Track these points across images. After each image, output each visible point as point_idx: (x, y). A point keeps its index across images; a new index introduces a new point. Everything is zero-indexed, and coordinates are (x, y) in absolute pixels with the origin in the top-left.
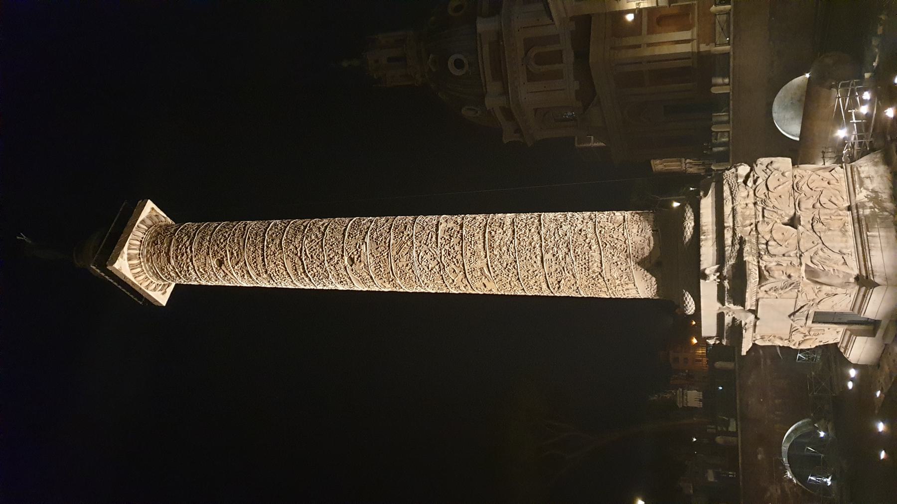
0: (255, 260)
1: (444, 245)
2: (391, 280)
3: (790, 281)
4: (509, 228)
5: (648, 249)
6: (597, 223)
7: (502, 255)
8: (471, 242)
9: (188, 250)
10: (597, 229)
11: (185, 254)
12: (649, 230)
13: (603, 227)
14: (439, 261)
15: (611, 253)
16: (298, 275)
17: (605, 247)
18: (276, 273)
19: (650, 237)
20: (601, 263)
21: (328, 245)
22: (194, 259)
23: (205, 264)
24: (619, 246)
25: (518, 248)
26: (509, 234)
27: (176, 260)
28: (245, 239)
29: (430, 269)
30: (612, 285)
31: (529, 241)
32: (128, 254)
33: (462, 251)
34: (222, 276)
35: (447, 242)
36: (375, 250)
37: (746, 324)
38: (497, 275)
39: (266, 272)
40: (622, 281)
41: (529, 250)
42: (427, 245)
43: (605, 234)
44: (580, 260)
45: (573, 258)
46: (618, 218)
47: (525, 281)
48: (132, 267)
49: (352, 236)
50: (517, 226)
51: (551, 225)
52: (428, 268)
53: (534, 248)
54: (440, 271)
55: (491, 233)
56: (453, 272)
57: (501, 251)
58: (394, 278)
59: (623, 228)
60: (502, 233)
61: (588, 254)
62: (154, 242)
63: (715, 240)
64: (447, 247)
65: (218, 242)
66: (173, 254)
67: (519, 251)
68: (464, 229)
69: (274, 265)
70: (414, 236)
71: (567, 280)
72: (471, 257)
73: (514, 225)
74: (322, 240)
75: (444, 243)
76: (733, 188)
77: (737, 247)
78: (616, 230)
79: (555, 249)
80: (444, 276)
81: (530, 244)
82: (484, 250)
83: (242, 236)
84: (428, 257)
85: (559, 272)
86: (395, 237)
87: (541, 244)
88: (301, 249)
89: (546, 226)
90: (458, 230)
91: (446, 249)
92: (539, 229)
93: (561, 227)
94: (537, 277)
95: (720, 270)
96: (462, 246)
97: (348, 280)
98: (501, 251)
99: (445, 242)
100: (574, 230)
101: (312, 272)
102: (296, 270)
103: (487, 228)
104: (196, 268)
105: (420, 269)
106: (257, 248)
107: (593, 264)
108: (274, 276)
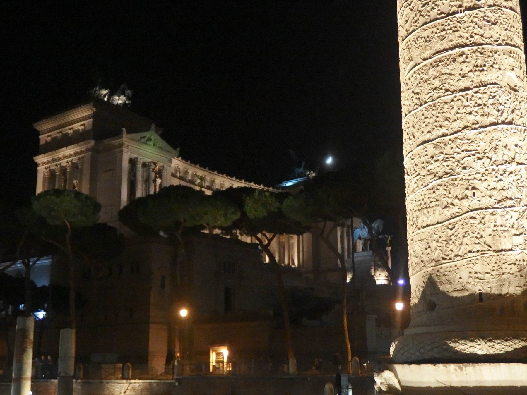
4: (472, 81)
6: (491, 211)
7: (429, 82)
8: (444, 30)
10: (478, 212)
12: (480, 288)
13: (483, 221)
15: (440, 237)
17: (448, 228)
19: (467, 290)
20: (428, 226)
25: (439, 102)
31: (451, 116)
33: (431, 22)
41: (437, 119)
43: (469, 226)
44: (430, 196)
50: (477, 92)
51: (482, 144)
53: (441, 127)
55: (461, 55)
59: (485, 251)
60: (461, 72)
63: (448, 385)
67: (434, 106)
68: (467, 12)
78: (477, 241)
79: (441, 157)
87: (447, 135)
89: (481, 136)
90: (465, 5)
92: (474, 126)
93: (479, 159)
96: (437, 19)
98: (434, 79)
100: (475, 178)
103: (470, 48)
107: (425, 214)
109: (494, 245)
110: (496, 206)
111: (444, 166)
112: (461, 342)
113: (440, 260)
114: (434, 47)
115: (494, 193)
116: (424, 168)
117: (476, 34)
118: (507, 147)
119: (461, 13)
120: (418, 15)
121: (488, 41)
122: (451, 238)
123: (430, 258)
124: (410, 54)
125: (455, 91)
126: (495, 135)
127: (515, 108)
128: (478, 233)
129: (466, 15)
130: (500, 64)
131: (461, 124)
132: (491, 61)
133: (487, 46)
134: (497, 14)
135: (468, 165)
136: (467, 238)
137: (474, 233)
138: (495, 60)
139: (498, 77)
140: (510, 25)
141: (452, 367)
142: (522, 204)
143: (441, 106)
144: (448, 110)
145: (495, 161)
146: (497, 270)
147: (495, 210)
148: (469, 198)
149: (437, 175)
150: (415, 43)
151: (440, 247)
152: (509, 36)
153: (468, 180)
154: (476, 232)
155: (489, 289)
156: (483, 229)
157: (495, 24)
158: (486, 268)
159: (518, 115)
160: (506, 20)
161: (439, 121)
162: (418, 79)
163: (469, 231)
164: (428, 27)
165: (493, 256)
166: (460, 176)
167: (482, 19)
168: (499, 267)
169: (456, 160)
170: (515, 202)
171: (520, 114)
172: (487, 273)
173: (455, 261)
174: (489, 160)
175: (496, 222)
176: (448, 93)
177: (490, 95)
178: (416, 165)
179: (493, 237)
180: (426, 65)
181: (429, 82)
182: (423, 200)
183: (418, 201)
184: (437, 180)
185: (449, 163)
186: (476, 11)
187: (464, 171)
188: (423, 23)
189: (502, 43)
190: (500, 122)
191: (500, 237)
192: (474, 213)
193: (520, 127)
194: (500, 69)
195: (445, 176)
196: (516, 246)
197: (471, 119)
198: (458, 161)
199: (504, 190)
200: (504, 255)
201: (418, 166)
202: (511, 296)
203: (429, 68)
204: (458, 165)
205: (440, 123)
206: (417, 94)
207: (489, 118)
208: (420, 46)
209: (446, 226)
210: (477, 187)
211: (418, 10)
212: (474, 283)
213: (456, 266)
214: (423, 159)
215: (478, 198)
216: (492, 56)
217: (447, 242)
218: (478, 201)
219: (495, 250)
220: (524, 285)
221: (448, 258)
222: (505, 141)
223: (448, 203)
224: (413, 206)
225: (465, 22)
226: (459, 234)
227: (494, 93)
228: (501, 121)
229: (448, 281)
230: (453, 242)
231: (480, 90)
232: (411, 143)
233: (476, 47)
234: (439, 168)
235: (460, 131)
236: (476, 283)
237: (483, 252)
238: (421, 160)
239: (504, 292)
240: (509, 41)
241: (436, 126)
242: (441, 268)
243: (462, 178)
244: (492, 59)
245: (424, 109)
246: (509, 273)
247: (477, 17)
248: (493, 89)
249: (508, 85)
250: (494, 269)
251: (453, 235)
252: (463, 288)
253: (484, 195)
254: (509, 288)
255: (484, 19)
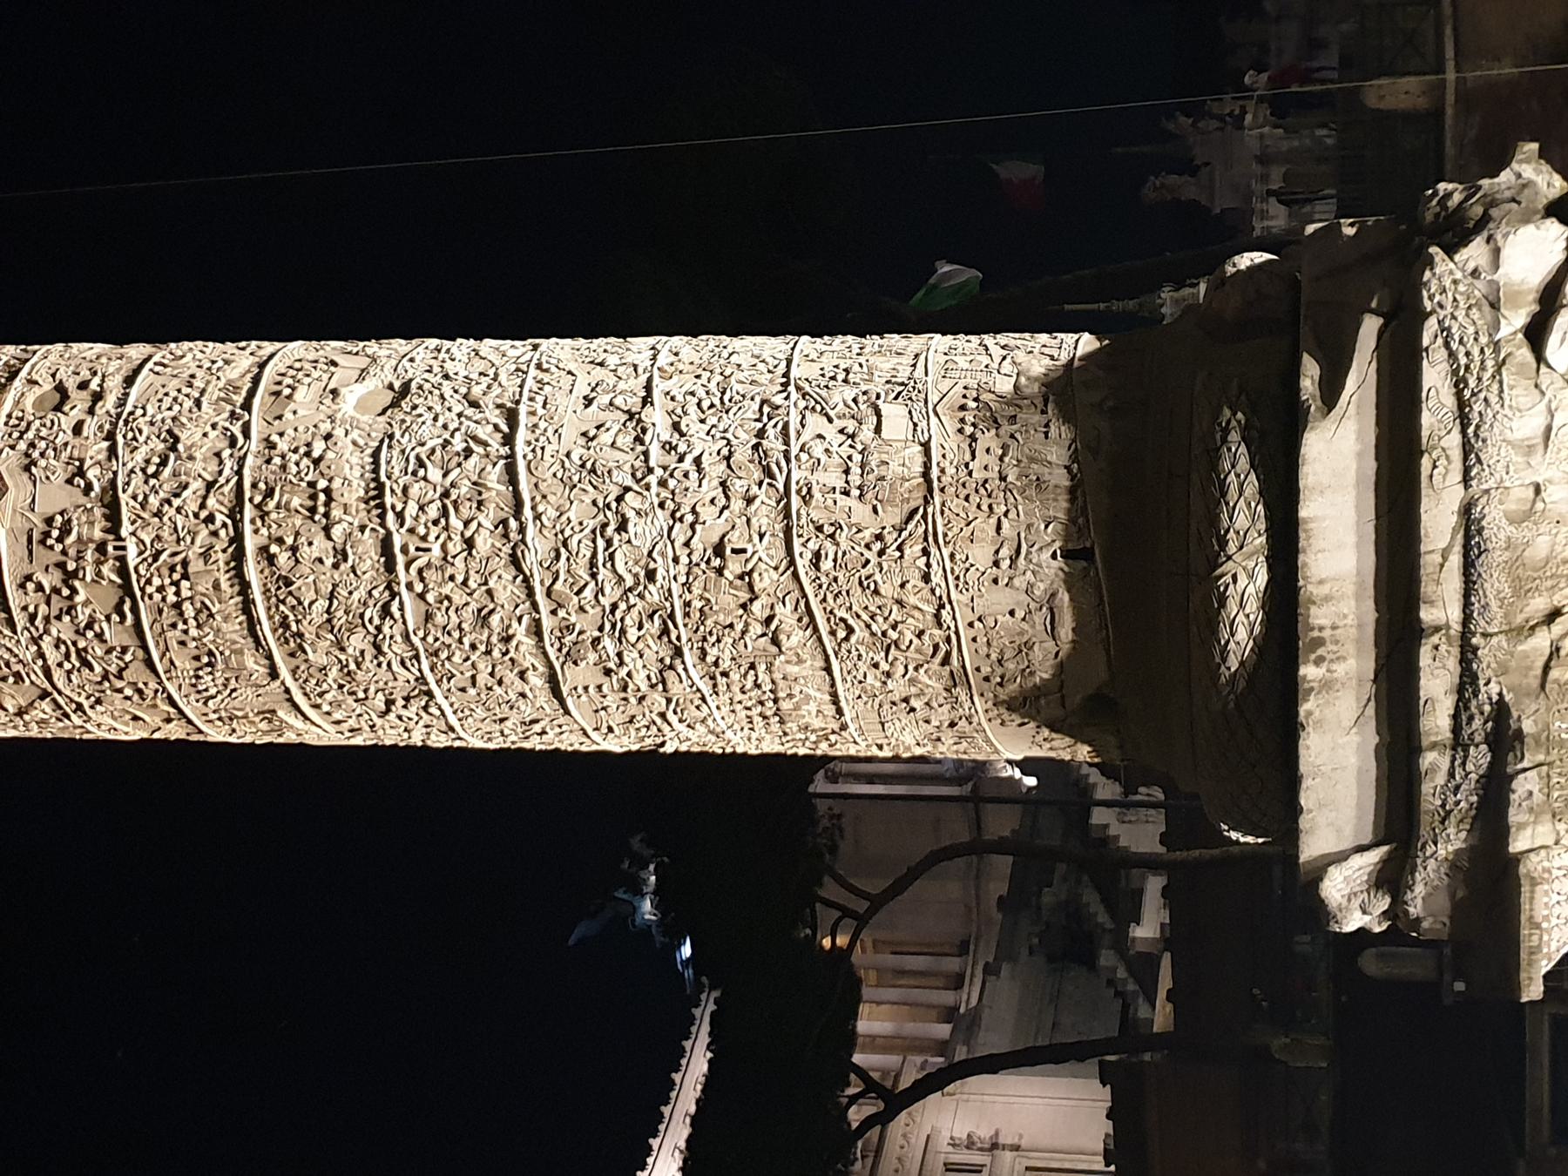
1: (47, 619)
4: (362, 528)
6: (795, 501)
7: (353, 666)
8: (177, 606)
10: (797, 542)
12: (1046, 555)
13: (828, 530)
15: (876, 666)
17: (847, 639)
19: (1053, 595)
24: (909, 636)
31: (474, 606)
41: (483, 648)
43: (841, 576)
45: (701, 684)
46: (895, 468)
50: (400, 516)
53: (507, 639)
55: (271, 559)
57: (343, 649)
59: (926, 531)
60: (329, 562)
64: (62, 629)
67: (436, 654)
72: (198, 677)
75: (43, 609)
78: (892, 552)
79: (608, 644)
87: (537, 623)
90: (98, 534)
92: (514, 536)
93: (622, 527)
98: (343, 649)
99: (48, 603)
100: (687, 544)
103: (248, 529)
109: (908, 500)
110: (781, 487)
111: (639, 638)
113: (952, 672)
114: (234, 642)
115: (738, 486)
116: (642, 698)
117: (203, 506)
118: (591, 434)
119: (124, 548)
120: (119, 684)
121: (229, 465)
122: (880, 634)
123: (942, 701)
124: (251, 715)
125: (389, 587)
126: (548, 468)
127: (465, 397)
128: (868, 546)
129: (133, 534)
130: (314, 435)
131: (505, 575)
132: (297, 464)
133: (246, 472)
134: (140, 432)
135: (642, 563)
136: (880, 582)
137: (868, 562)
138: (295, 451)
139: (354, 443)
140: (186, 390)
142: (778, 400)
143: (439, 635)
144: (452, 612)
145: (633, 475)
146: (989, 496)
147: (794, 487)
148: (750, 566)
149: (668, 661)
150: (213, 697)
151: (906, 667)
152: (222, 395)
154: (862, 555)
155: (1051, 526)
156: (855, 530)
157: (177, 440)
158: (983, 531)
159: (489, 387)
160: (167, 402)
161: (488, 642)
162: (340, 698)
163: (857, 575)
164: (164, 655)
165: (943, 504)
166: (676, 589)
167: (152, 481)
168: (982, 491)
169: (621, 599)
170: (773, 422)
171: (485, 381)
172: (999, 528)
173: (956, 627)
174: (629, 496)
175: (834, 489)
176: (394, 607)
177: (414, 473)
178: (631, 722)
179: (880, 501)
182: (748, 709)
183: (751, 722)
184: (683, 662)
186: (124, 498)
187: (659, 577)
188: (148, 671)
189: (240, 423)
190: (505, 451)
191: (882, 478)
192: (801, 554)
193: (530, 383)
194: (328, 437)
195: (673, 637)
196: (915, 430)
197: (490, 541)
198: (625, 593)
199: (730, 452)
200: (943, 471)
201: (634, 717)
202: (1074, 458)
203: (306, 661)
204: (639, 595)
205: (494, 639)
206: (389, 703)
207: (490, 485)
208: (225, 686)
209: (839, 645)
210: (716, 539)
211: (100, 683)
212: (1029, 573)
214: (612, 700)
215: (750, 540)
216: (283, 457)
217: (893, 647)
218: (761, 540)
219: (925, 497)
220: (1043, 412)
221: (943, 648)
222: (570, 435)
223: (764, 635)
224: (768, 737)
225: (158, 538)
226: (866, 608)
227: (407, 460)
228: (504, 445)
229: (1021, 651)
230: (894, 627)
231: (393, 507)
232: (558, 730)
233: (248, 506)
234: (647, 652)
235: (526, 580)
236: (1031, 567)
237: (930, 538)
238: (615, 706)
239: (1061, 478)
240: (239, 399)
241: (504, 654)
243: (683, 585)
244: (295, 457)
245: (445, 685)
246: (1001, 459)
247: (146, 497)
248: (393, 462)
249: (383, 412)
250: (985, 507)
251: (868, 626)
252: (1044, 609)
253: (744, 518)
254: (1050, 463)
255: (155, 475)
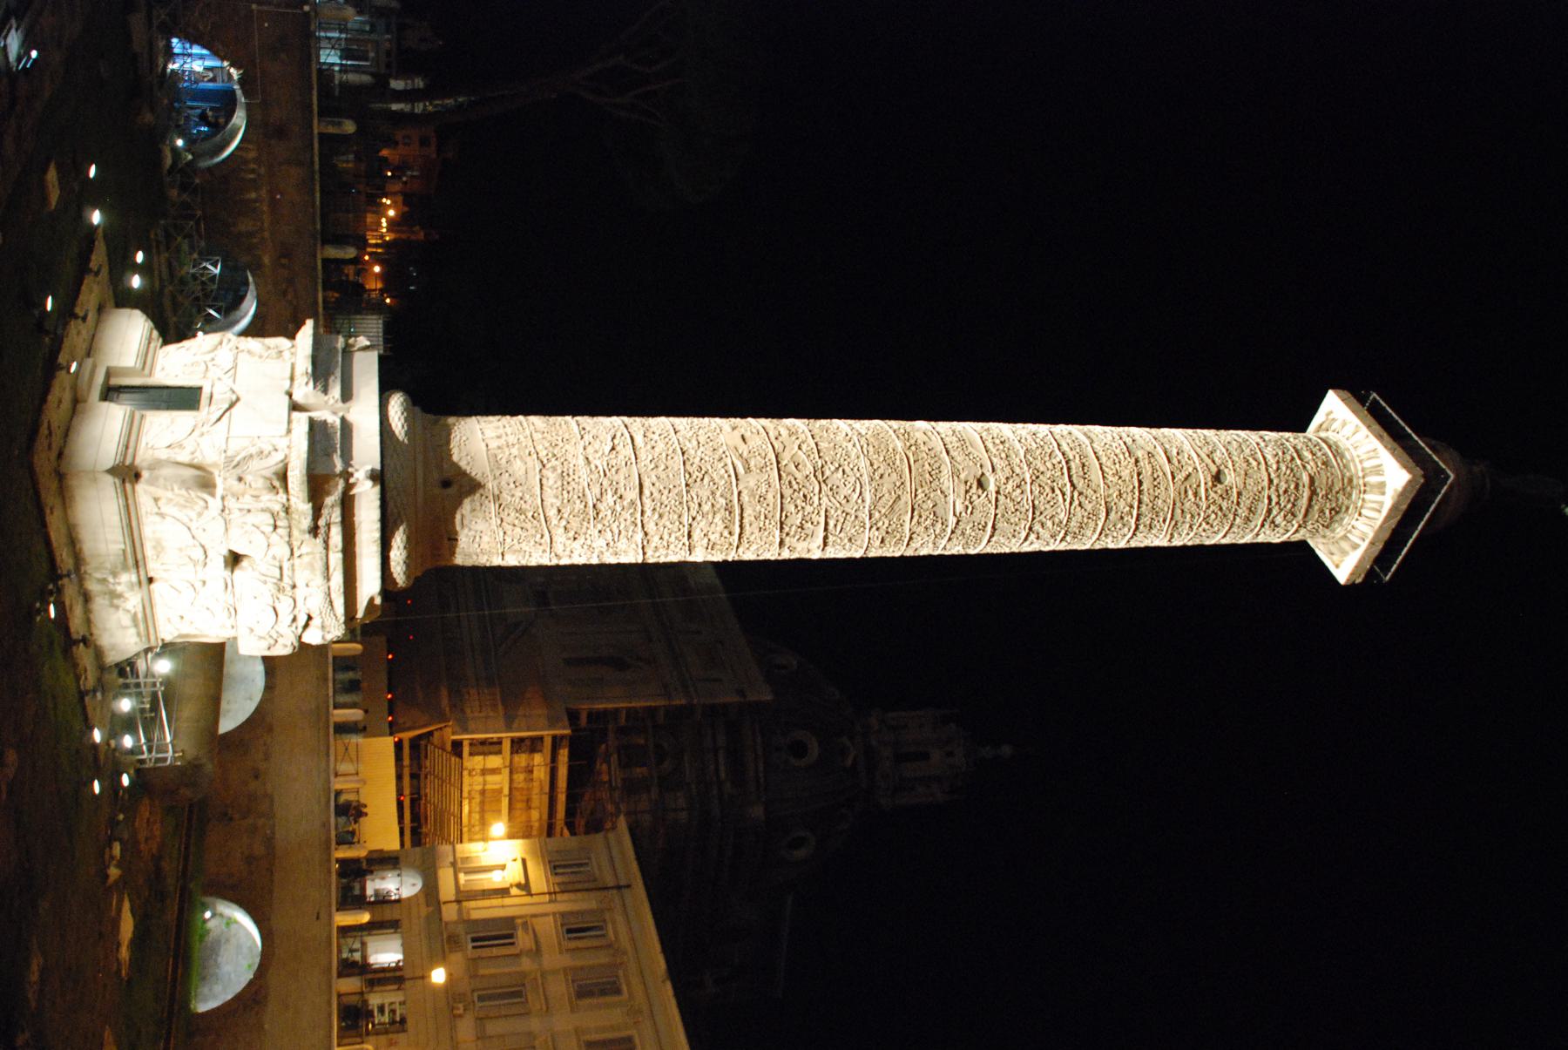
0: (1155, 483)
1: (813, 513)
2: (913, 448)
3: (238, 471)
5: (466, 510)
7: (711, 497)
8: (766, 518)
9: (1275, 500)
11: (1281, 492)
14: (823, 485)
16: (1080, 456)
18: (1119, 459)
20: (541, 485)
21: (1023, 510)
22: (1266, 483)
23: (1246, 474)
26: (698, 531)
27: (1299, 481)
28: (1172, 519)
29: (841, 469)
30: (524, 444)
32: (1383, 494)
33: (782, 503)
34: (1218, 452)
35: (808, 519)
36: (938, 502)
37: (307, 383)
38: (721, 459)
39: (1137, 461)
40: (507, 453)
41: (663, 506)
42: (843, 512)
47: (671, 449)
48: (1377, 470)
49: (980, 526)
52: (844, 471)
53: (654, 509)
54: (823, 466)
55: (730, 533)
56: (799, 464)
58: (907, 452)
60: (710, 533)
61: (563, 500)
62: (1337, 513)
65: (1219, 513)
66: (1303, 492)
67: (680, 503)
69: (1122, 474)
70: (868, 526)
71: (600, 453)
73: (689, 546)
74: (1033, 519)
75: (813, 516)
76: (329, 611)
77: (322, 522)
79: (618, 508)
80: (817, 457)
81: (661, 516)
82: (742, 506)
83: (1176, 524)
84: (845, 491)
85: (613, 467)
86: (902, 525)
88: (1071, 504)
89: (634, 546)
91: (811, 505)
94: (650, 458)
95: (349, 487)
97: (990, 446)
100: (586, 539)
101: (1055, 461)
102: (1083, 465)
104: (1263, 467)
105: (858, 470)
106: (1151, 505)
108: (1124, 454)
112: (404, 538)
141: (377, 535)
153: (586, 534)
180: (732, 494)
181: (711, 497)
185: (609, 517)
213: (491, 518)
230: (517, 518)
242: (490, 501)
